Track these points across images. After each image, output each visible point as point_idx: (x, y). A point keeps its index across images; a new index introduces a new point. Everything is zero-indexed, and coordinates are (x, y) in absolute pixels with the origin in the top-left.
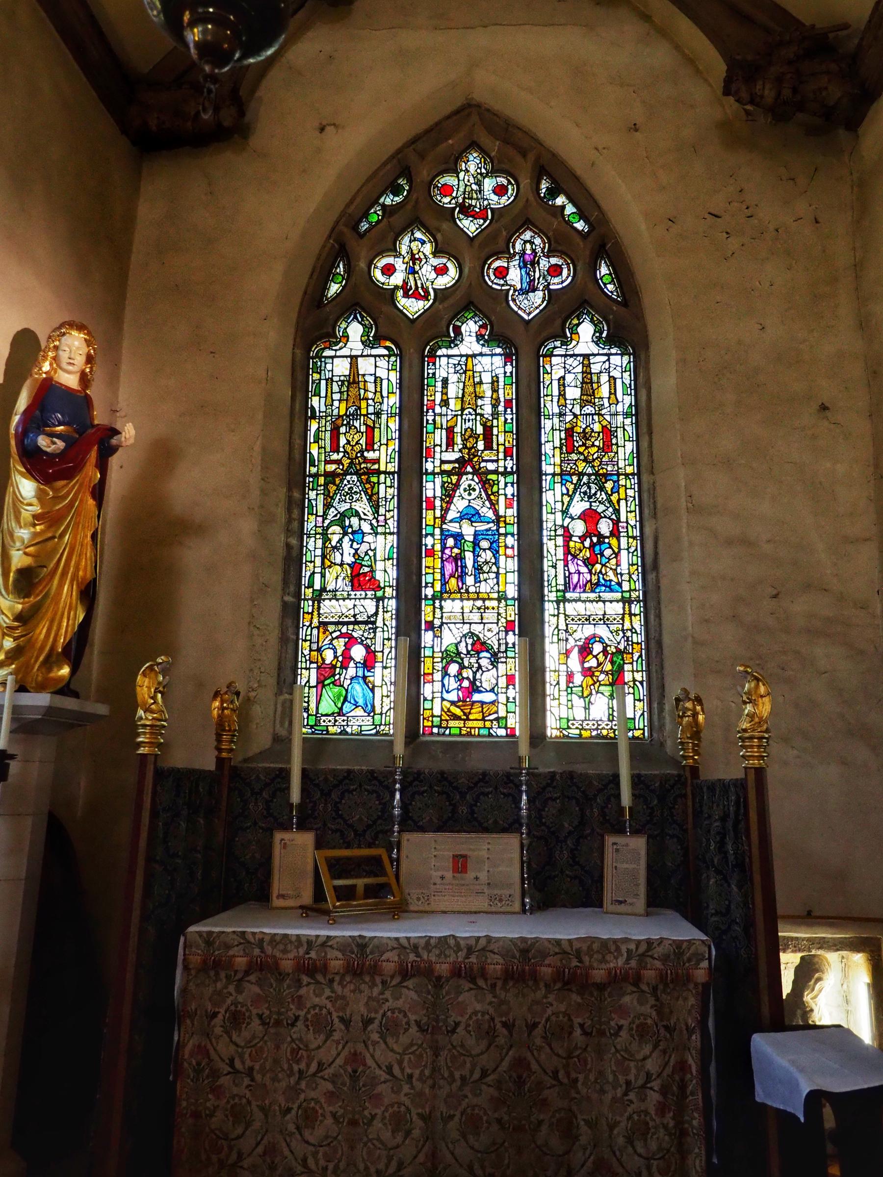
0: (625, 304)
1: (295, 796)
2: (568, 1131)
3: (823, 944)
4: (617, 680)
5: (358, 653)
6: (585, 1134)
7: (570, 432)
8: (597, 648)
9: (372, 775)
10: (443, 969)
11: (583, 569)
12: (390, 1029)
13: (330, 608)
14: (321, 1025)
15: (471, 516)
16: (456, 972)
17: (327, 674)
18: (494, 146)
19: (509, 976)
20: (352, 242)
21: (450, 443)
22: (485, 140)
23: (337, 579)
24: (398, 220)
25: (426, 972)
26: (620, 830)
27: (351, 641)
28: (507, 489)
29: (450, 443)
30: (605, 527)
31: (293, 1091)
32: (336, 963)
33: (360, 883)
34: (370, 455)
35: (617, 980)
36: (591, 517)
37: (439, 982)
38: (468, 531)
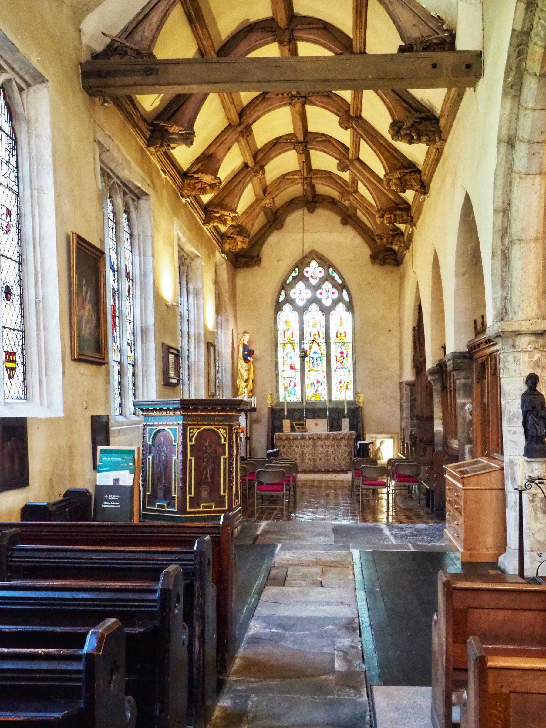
0: (349, 302)
1: (286, 413)
2: (335, 460)
3: (384, 438)
4: (347, 388)
5: (292, 384)
6: (337, 460)
7: (337, 333)
8: (343, 382)
9: (299, 409)
10: (315, 438)
11: (340, 364)
12: (307, 447)
13: (286, 375)
14: (297, 447)
15: (315, 353)
16: (318, 438)
17: (286, 388)
18: (319, 261)
19: (326, 439)
20: (285, 287)
21: (310, 336)
22: (316, 258)
23: (287, 368)
24: (296, 280)
25: (313, 439)
26: (345, 417)
27: (291, 381)
28: (324, 346)
29: (310, 336)
30: (344, 355)
31: (293, 456)
32: (299, 438)
33: (300, 427)
34: (292, 339)
35: (342, 439)
36: (342, 353)
37: (315, 440)
38: (315, 356)
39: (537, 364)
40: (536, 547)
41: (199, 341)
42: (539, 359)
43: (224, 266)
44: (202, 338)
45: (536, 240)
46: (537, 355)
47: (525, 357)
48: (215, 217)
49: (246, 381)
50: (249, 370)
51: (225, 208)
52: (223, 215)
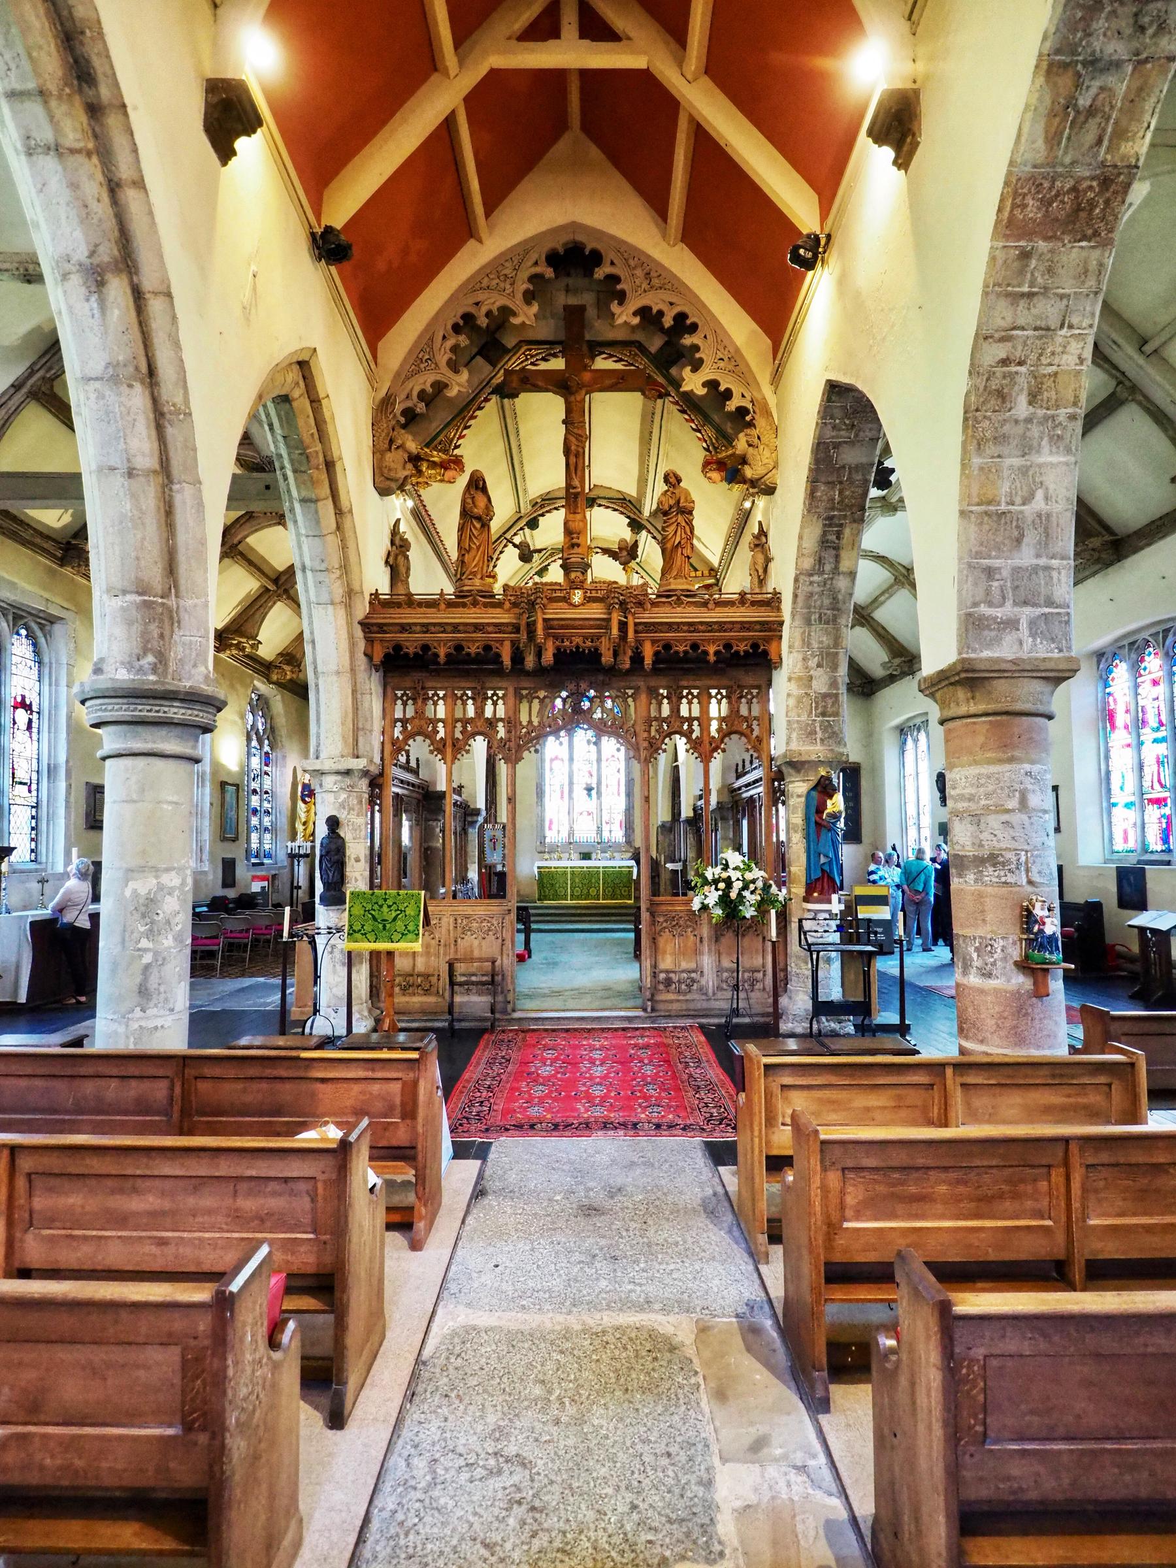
39: (342, 806)
40: (333, 1002)
41: (203, 782)
42: (344, 801)
43: (279, 697)
44: (208, 777)
45: (338, 673)
46: (343, 796)
47: (330, 798)
48: (232, 645)
49: (304, 824)
50: (308, 811)
51: (242, 636)
52: (240, 642)
